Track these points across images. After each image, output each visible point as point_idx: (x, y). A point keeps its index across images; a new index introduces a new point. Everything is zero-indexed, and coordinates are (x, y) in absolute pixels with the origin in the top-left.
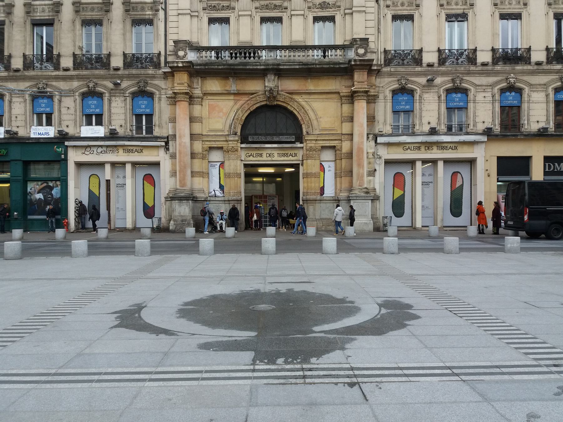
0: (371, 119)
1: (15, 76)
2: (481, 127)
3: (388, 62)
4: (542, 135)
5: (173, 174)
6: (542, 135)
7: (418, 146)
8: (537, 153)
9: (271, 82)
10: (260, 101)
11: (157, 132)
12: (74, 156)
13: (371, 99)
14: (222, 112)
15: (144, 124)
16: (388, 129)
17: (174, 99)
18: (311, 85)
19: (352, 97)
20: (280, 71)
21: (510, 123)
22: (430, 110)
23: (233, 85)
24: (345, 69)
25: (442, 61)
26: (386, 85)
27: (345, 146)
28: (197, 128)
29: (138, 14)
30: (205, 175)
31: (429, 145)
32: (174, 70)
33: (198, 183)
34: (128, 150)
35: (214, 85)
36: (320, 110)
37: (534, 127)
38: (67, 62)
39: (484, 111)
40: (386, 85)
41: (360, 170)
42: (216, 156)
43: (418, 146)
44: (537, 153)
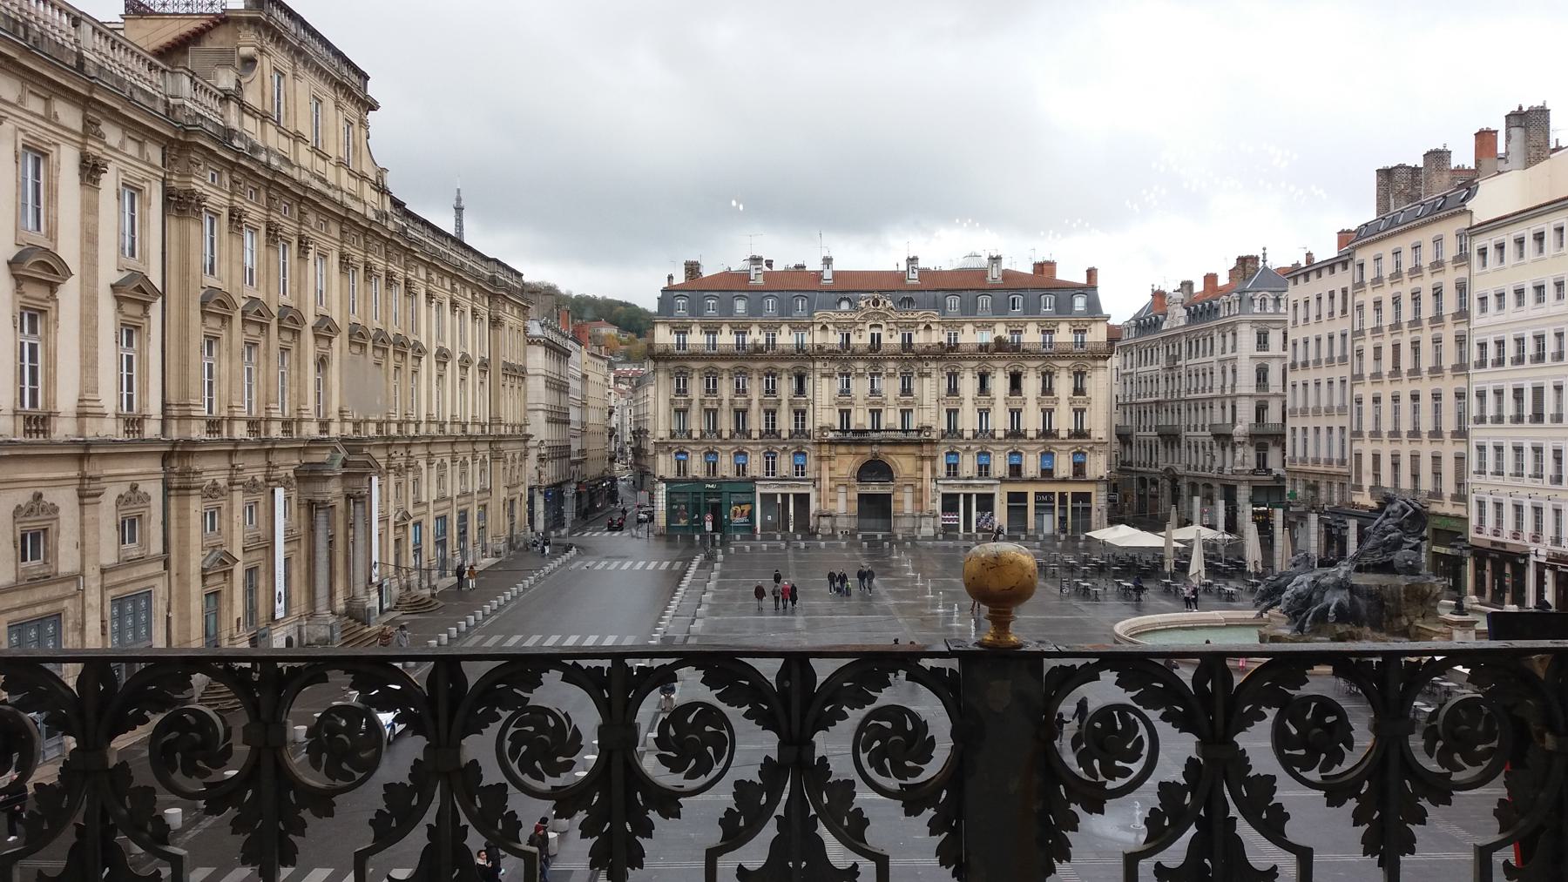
0: (934, 470)
1: (726, 442)
2: (998, 475)
3: (943, 436)
4: (1032, 480)
5: (819, 500)
6: (1032, 480)
7: (961, 486)
8: (1031, 490)
9: (875, 449)
10: (869, 458)
11: (808, 476)
12: (759, 490)
13: (933, 459)
14: (846, 464)
15: (800, 469)
16: (944, 475)
17: (820, 458)
18: (898, 450)
19: (922, 458)
20: (879, 443)
21: (1016, 470)
22: (968, 465)
23: (853, 449)
24: (919, 441)
25: (975, 436)
26: (942, 451)
27: (919, 485)
28: (834, 474)
29: (798, 407)
30: (835, 500)
31: (967, 485)
32: (820, 444)
33: (831, 506)
34: (791, 486)
35: (842, 449)
36: (903, 464)
37: (1029, 475)
38: (755, 435)
39: (1000, 466)
40: (942, 451)
41: (927, 501)
42: (842, 489)
43: (961, 486)
44: (1031, 490)
